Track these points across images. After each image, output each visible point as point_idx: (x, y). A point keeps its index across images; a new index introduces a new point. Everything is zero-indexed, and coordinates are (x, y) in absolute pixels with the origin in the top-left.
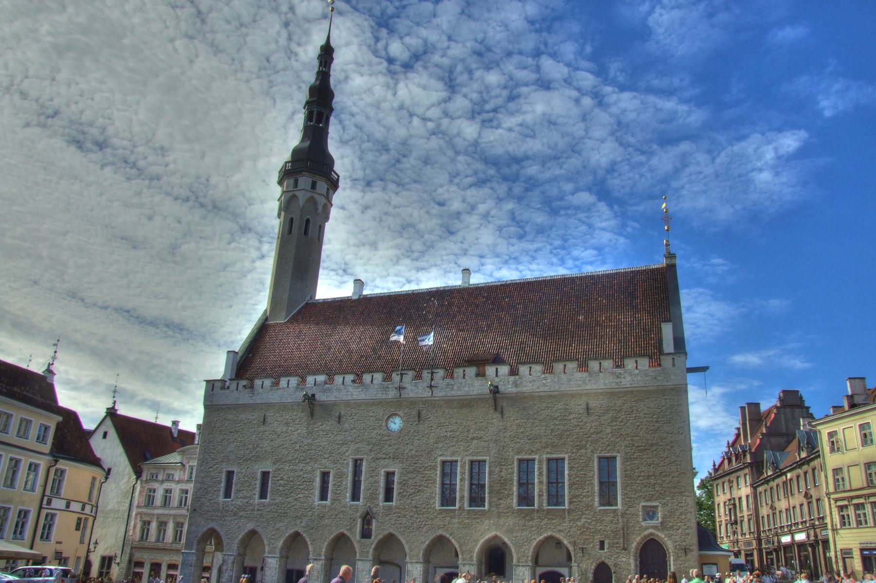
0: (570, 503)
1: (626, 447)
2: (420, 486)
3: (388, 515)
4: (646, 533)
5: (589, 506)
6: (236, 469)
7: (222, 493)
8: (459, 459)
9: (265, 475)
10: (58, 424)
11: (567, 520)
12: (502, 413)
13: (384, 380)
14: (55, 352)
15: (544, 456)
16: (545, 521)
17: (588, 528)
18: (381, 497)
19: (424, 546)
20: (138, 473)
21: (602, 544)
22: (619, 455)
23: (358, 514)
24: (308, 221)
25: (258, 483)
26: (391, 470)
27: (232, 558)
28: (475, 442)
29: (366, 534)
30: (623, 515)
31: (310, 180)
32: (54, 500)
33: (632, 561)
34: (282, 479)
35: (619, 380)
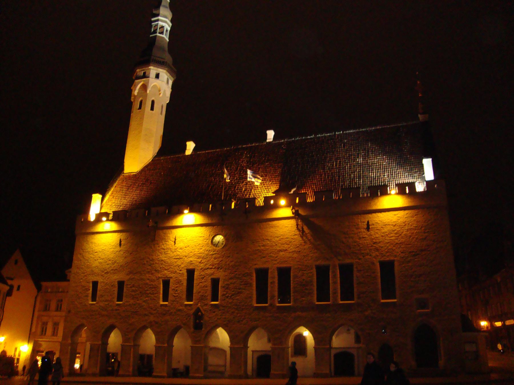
0: (359, 298)
1: (402, 253)
3: (214, 312)
6: (100, 279)
15: (337, 263)
18: (209, 297)
20: (39, 288)
22: (396, 259)
23: (192, 312)
24: (153, 102)
25: (116, 289)
26: (215, 276)
28: (281, 253)
34: (133, 286)
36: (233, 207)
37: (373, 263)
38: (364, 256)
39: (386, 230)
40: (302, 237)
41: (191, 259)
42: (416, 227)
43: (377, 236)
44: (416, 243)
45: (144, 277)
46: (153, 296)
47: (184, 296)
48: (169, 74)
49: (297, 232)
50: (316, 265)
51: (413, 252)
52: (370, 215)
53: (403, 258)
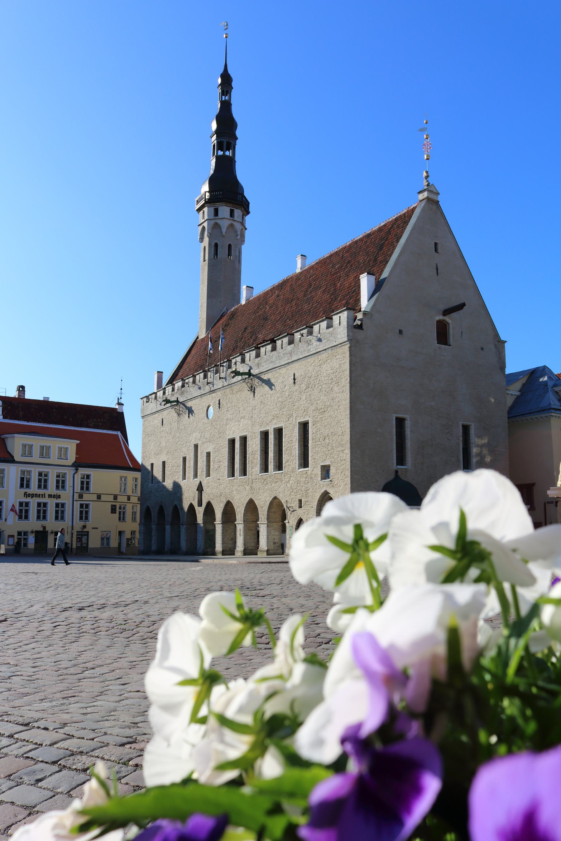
4: (323, 491)
7: (150, 481)
9: (164, 463)
10: (77, 445)
11: (284, 482)
12: (254, 392)
13: (205, 377)
14: (121, 389)
19: (221, 510)
21: (300, 501)
24: (216, 245)
26: (208, 451)
27: (155, 526)
28: (242, 420)
29: (200, 504)
31: (212, 209)
32: (84, 495)
35: (309, 347)
47: (192, 473)
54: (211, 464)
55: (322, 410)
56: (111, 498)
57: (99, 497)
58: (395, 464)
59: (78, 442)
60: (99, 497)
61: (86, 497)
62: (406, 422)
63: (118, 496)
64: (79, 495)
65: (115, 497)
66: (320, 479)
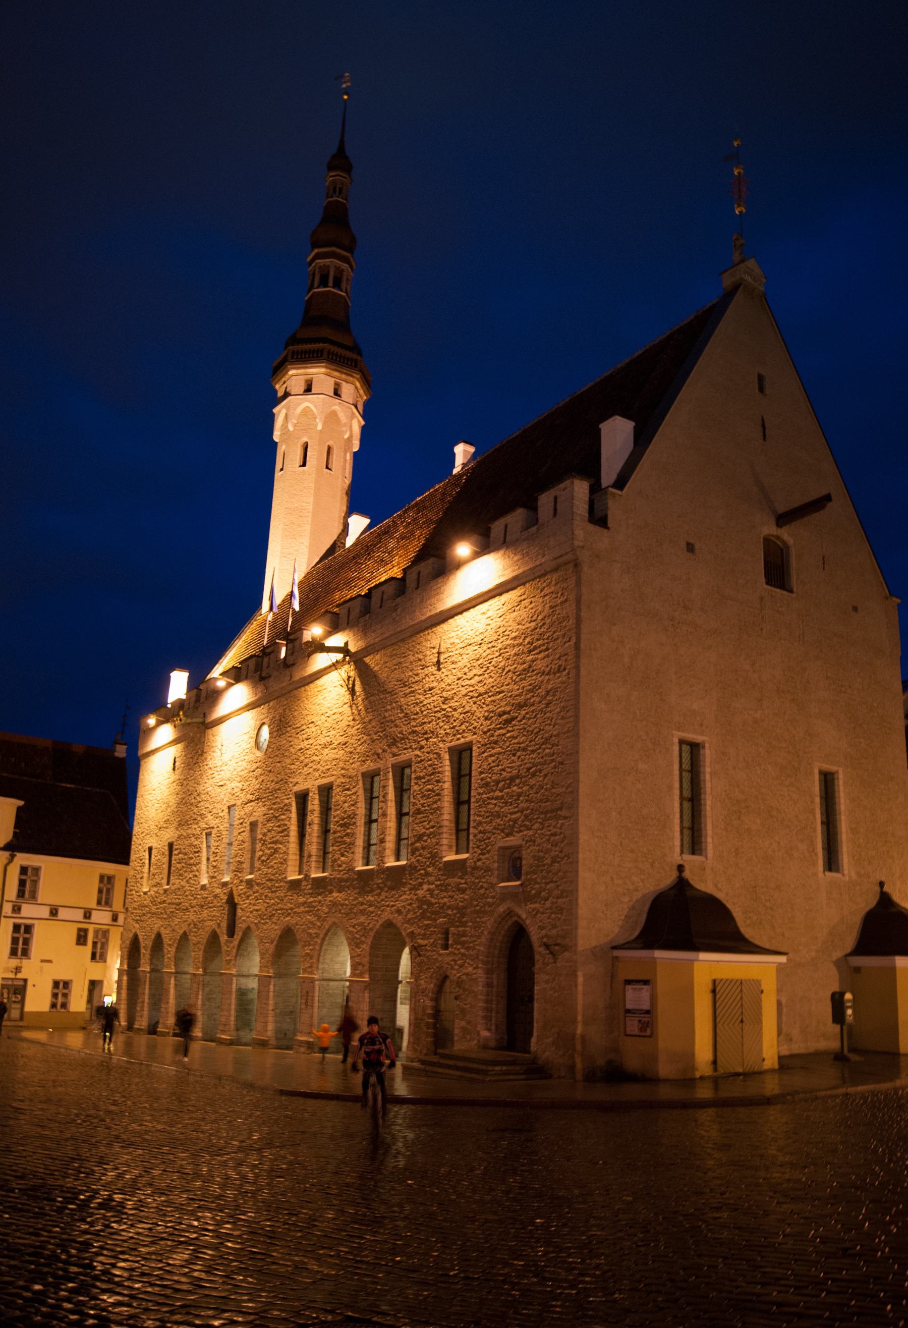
1: (486, 718)
2: (276, 842)
3: (248, 896)
4: (501, 909)
5: (435, 857)
6: (154, 845)
8: (310, 786)
10: (19, 809)
16: (384, 894)
17: (430, 904)
18: (246, 866)
21: (447, 933)
25: (166, 860)
28: (326, 751)
30: (475, 868)
33: (480, 974)
36: (283, 655)
37: (439, 755)
38: (427, 739)
39: (464, 661)
40: (351, 706)
41: (233, 785)
42: (515, 638)
43: (449, 680)
44: (510, 687)
45: (190, 831)
46: (195, 868)
48: (336, 374)
49: (347, 697)
50: (363, 774)
51: (505, 713)
52: (445, 626)
53: (485, 733)
54: (258, 846)
55: (505, 717)
56: (79, 915)
57: (54, 912)
58: (678, 850)
59: (21, 803)
60: (54, 912)
61: (28, 910)
62: (702, 752)
63: (94, 913)
64: (14, 907)
65: (87, 915)
66: (494, 880)
